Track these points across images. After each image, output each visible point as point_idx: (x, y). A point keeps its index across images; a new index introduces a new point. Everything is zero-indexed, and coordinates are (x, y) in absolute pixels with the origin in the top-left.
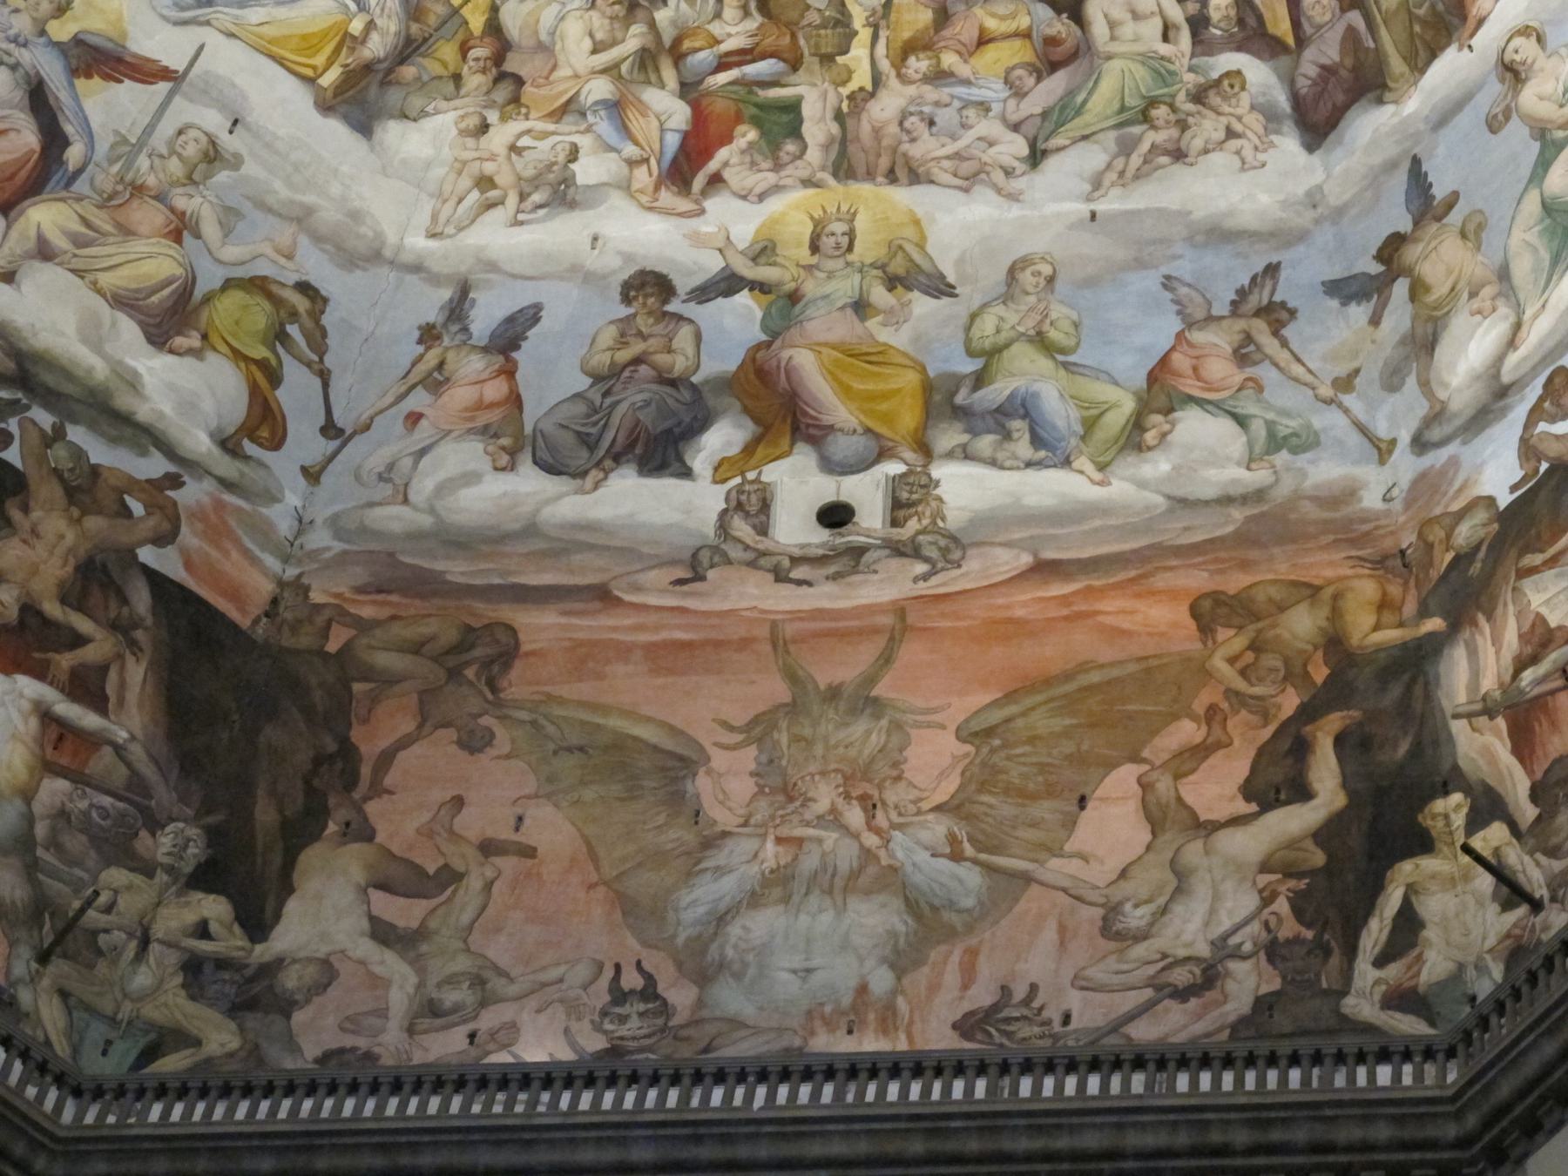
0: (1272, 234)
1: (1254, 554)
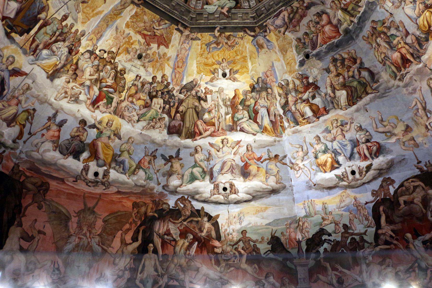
0: (159, 144)
1: (141, 196)
